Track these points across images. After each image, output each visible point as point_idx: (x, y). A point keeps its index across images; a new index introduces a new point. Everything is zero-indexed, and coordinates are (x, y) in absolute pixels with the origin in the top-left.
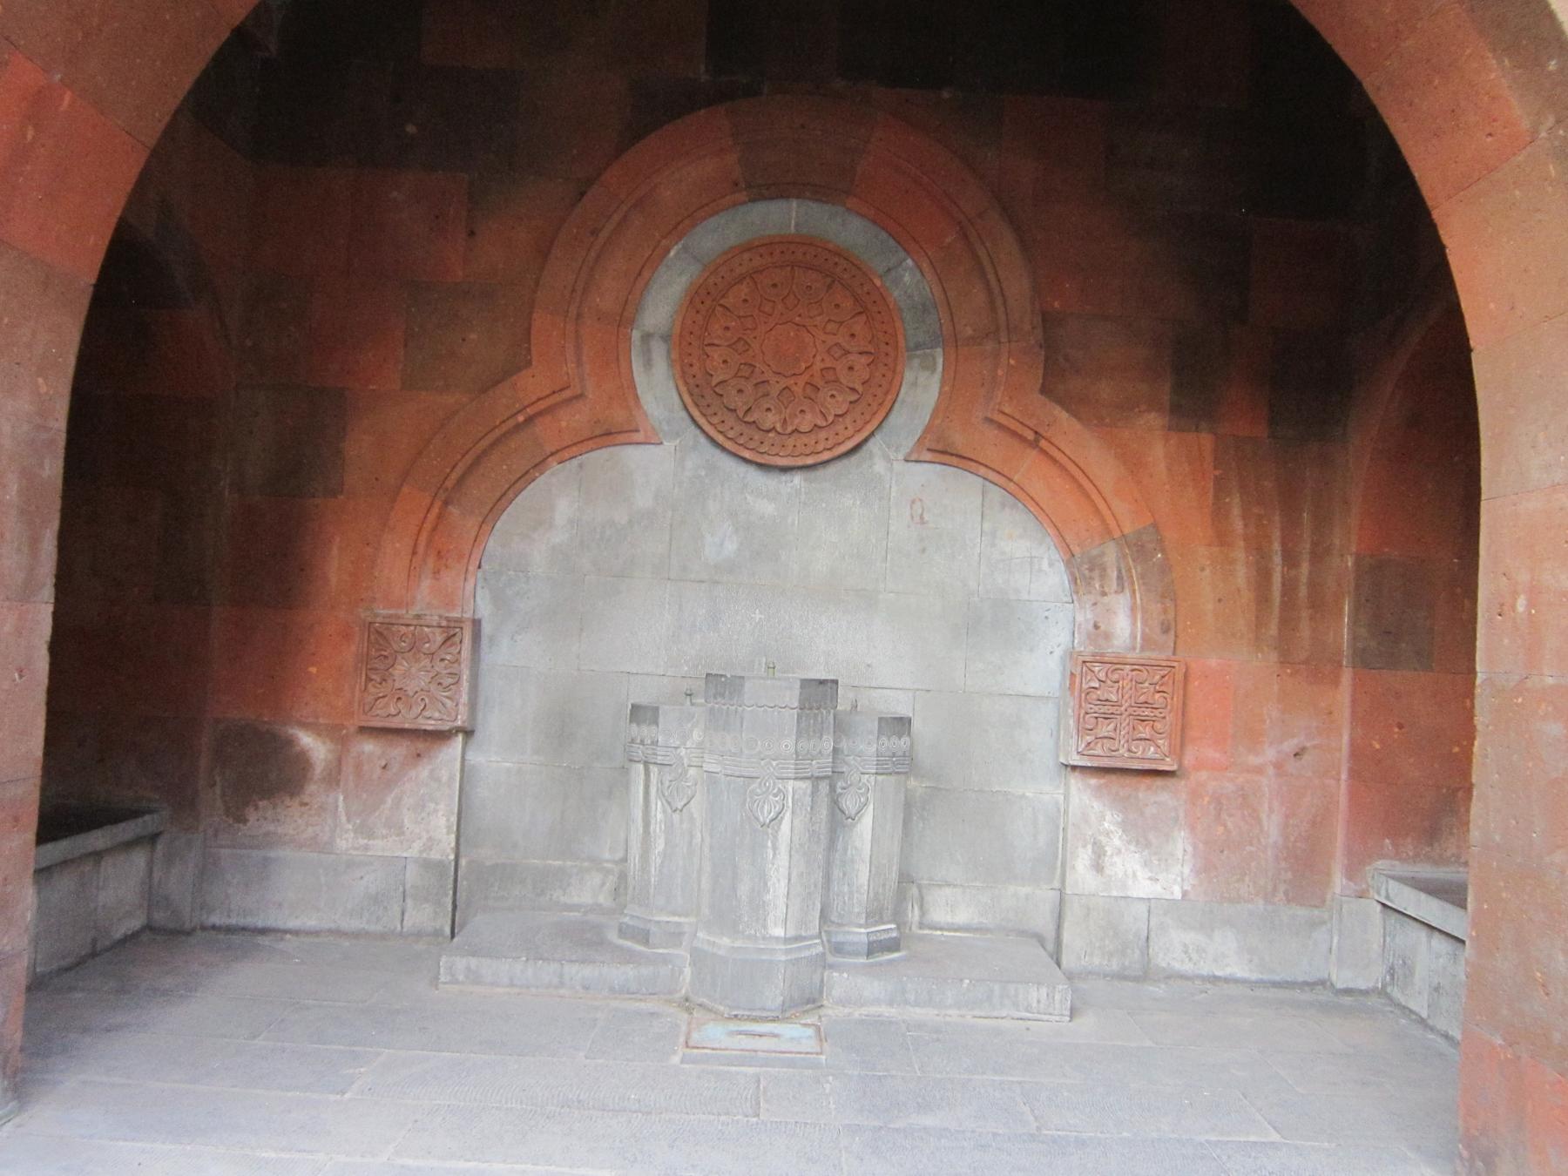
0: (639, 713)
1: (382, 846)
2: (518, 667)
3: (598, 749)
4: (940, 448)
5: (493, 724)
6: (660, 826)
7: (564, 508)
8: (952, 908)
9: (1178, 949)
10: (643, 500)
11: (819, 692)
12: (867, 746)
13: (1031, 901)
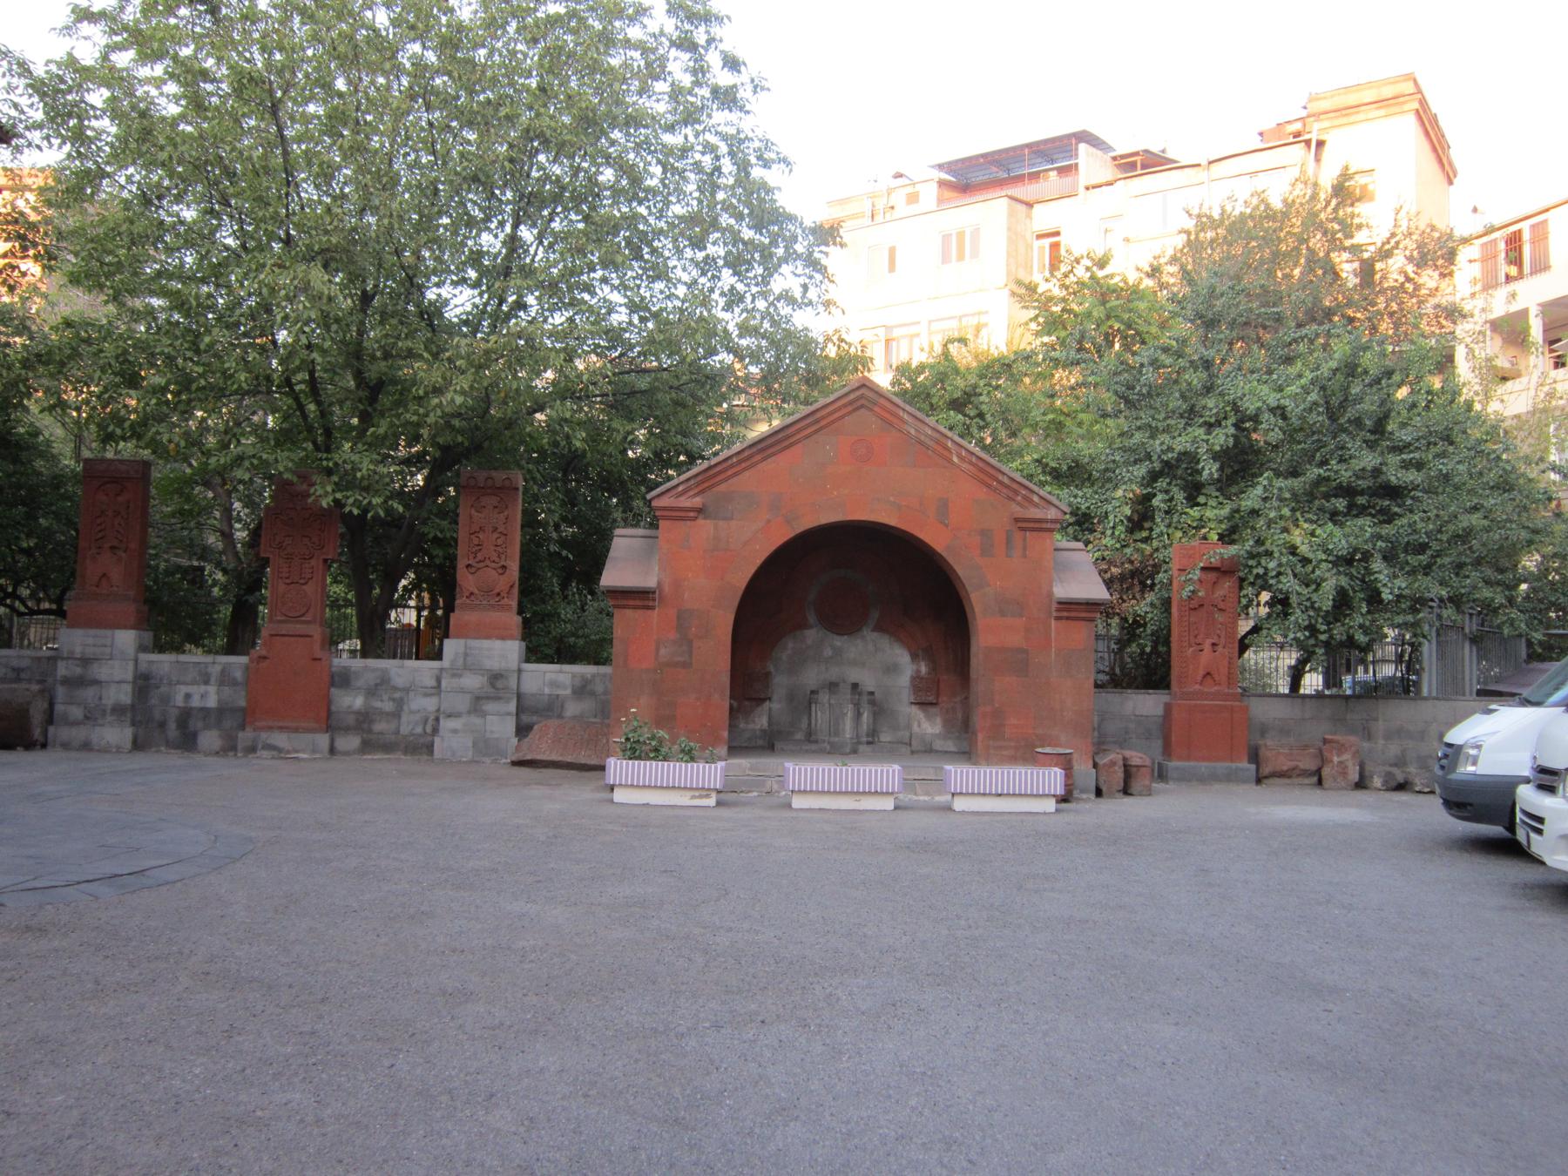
0: (812, 692)
1: (751, 726)
2: (781, 683)
3: (804, 702)
4: (879, 628)
5: (775, 697)
6: (821, 717)
7: (790, 645)
8: (885, 737)
9: (938, 745)
10: (809, 642)
11: (855, 686)
12: (865, 698)
13: (905, 734)
